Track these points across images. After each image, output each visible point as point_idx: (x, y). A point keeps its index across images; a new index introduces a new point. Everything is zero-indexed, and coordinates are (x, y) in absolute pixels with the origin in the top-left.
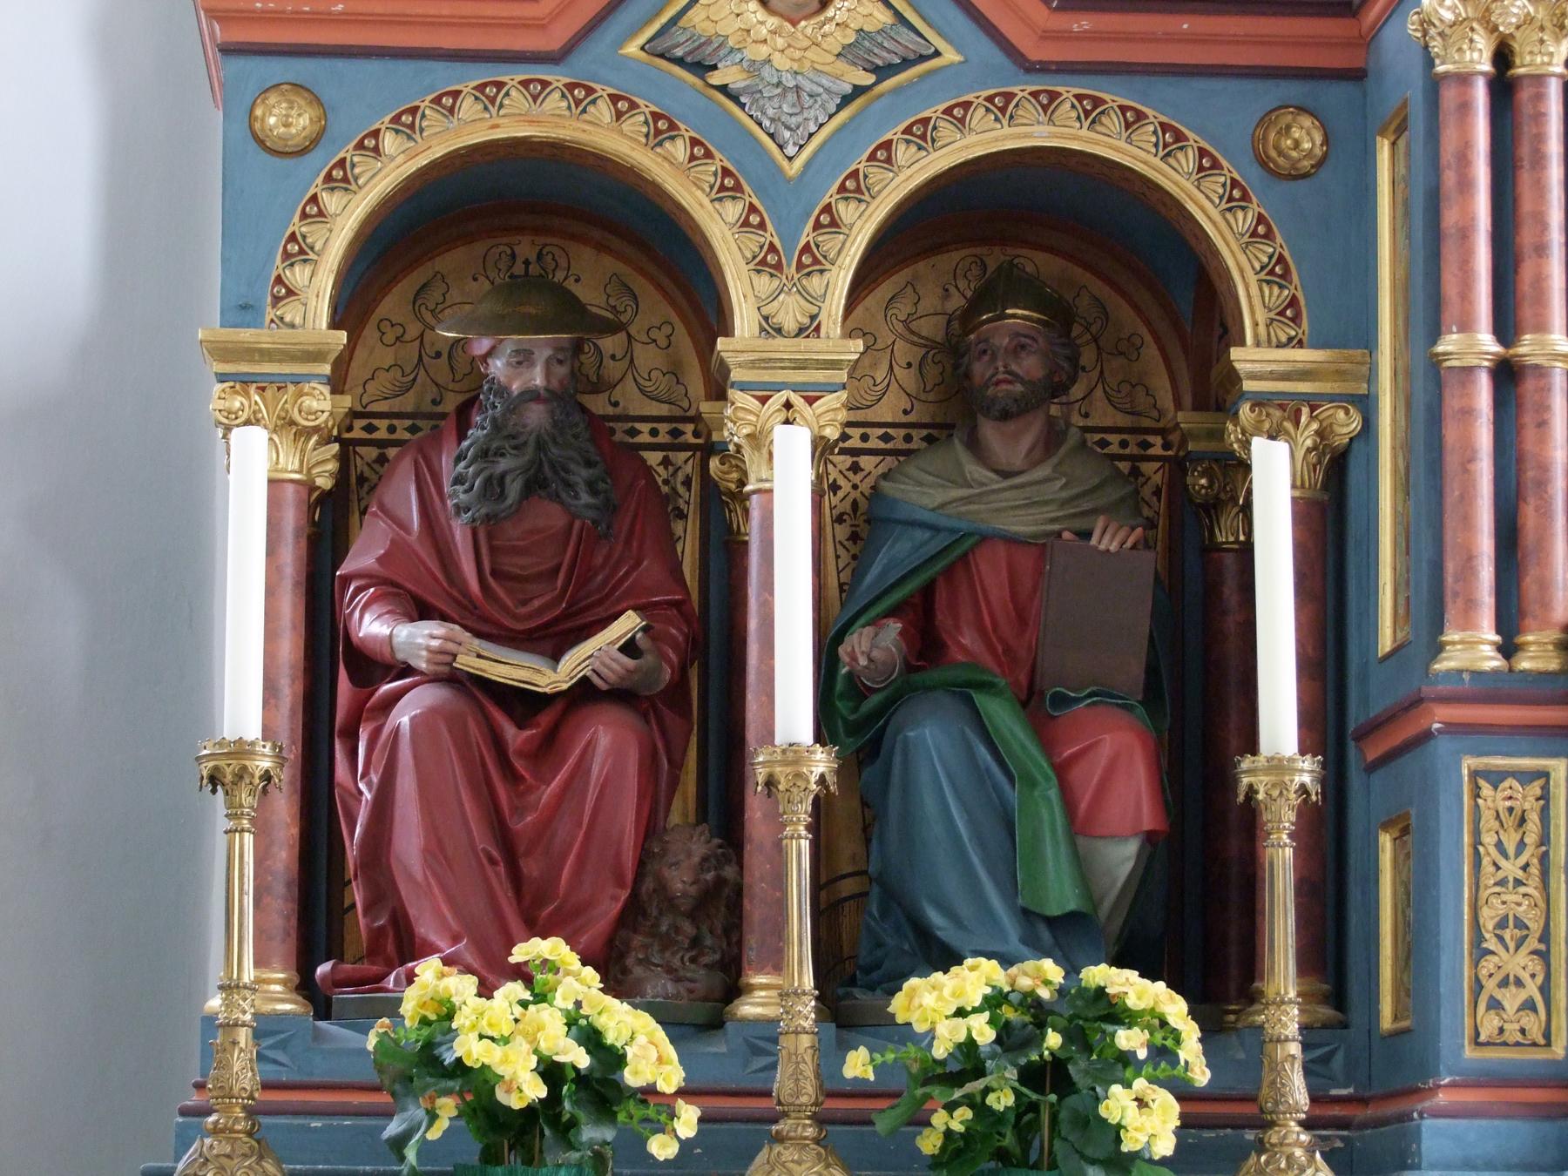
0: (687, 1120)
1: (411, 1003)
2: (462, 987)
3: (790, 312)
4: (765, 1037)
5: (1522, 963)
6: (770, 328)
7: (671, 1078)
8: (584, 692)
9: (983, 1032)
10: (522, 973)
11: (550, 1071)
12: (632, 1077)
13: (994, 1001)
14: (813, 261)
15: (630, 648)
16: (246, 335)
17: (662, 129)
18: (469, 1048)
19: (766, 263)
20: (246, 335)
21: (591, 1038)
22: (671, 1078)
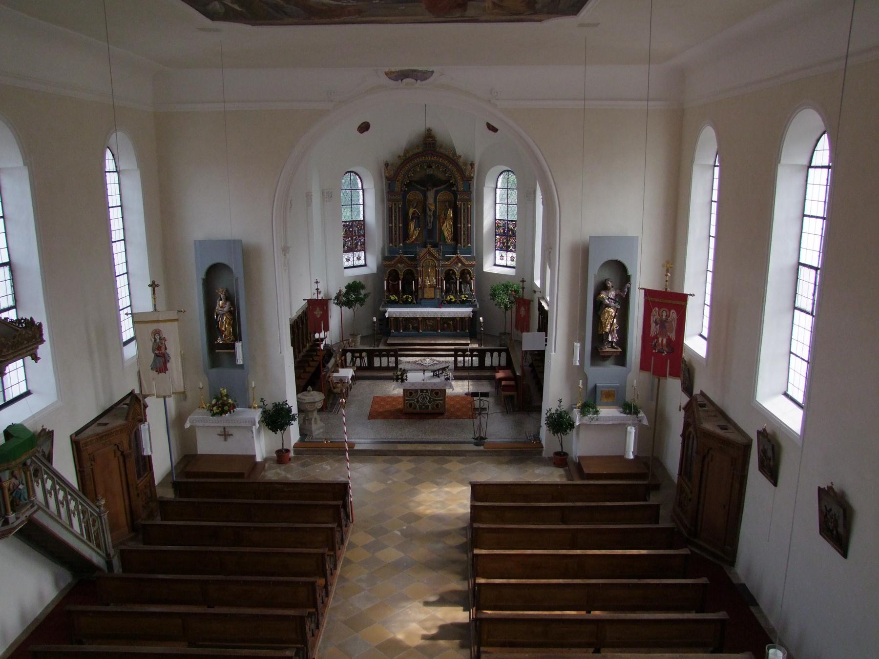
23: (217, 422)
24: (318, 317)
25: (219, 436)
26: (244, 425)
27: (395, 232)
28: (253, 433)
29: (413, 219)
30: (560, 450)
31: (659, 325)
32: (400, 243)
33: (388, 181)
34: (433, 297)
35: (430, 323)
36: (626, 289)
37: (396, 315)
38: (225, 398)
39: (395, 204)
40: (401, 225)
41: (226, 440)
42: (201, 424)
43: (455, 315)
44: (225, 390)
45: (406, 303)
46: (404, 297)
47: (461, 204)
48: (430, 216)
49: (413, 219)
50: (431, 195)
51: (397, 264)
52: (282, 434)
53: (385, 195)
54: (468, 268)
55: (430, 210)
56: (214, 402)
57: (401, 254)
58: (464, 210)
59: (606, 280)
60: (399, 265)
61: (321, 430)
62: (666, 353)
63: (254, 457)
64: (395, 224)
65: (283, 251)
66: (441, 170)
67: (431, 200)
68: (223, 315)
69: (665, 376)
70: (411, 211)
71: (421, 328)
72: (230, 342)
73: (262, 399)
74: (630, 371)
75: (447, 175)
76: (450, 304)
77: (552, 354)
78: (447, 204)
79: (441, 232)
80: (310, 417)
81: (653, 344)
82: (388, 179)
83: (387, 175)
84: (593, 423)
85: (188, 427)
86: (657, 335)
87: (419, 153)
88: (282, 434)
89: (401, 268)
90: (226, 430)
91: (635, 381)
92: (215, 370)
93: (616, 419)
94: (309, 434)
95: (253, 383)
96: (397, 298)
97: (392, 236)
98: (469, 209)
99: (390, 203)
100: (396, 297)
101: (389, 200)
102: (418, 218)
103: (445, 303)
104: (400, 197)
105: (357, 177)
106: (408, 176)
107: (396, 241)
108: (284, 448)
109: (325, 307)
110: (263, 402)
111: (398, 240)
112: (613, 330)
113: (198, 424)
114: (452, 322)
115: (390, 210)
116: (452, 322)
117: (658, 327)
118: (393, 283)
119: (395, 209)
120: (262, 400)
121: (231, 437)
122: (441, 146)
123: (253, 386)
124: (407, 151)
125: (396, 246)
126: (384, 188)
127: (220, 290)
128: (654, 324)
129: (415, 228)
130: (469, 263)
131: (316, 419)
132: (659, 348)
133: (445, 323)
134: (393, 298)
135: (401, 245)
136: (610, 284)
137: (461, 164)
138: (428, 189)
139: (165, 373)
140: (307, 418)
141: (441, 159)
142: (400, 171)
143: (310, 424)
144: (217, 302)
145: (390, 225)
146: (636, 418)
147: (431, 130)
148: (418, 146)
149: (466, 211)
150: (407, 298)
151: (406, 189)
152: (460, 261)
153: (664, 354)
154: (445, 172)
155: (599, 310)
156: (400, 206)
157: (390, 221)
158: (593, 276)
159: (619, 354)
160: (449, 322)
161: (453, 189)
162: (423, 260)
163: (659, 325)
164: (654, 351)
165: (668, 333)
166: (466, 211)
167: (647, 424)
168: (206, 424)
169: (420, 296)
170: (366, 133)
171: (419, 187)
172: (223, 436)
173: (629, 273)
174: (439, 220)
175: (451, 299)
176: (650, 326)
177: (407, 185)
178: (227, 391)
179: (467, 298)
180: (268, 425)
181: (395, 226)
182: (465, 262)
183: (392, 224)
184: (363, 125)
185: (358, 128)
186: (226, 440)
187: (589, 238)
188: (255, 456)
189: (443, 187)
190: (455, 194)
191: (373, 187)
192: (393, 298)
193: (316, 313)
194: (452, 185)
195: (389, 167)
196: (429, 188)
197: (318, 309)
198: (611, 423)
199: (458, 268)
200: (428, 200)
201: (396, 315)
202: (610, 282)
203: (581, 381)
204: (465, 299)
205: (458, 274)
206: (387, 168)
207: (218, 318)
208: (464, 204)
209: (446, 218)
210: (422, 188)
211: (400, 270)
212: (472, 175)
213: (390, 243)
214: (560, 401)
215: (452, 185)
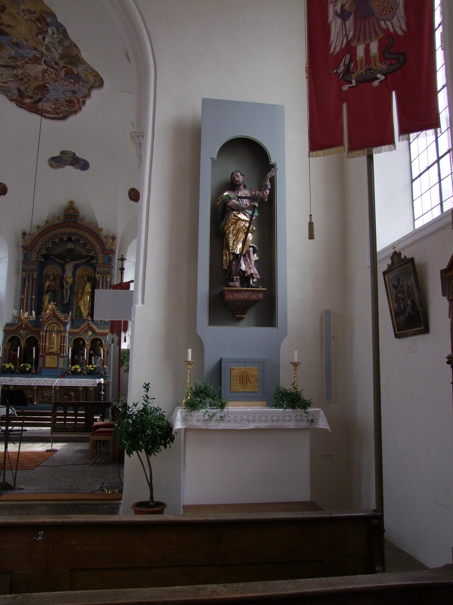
0: (13, 369)
5: (41, 364)
11: (9, 367)
14: (24, 340)
17: (19, 336)
19: (22, 340)
21: (10, 366)
27: (27, 303)
29: (47, 292)
30: (148, 499)
31: (352, 17)
33: (24, 250)
34: (56, 366)
35: (48, 394)
36: (268, 183)
39: (29, 275)
40: (34, 297)
43: (77, 384)
45: (23, 373)
46: (22, 365)
47: (100, 277)
48: (67, 290)
50: (69, 268)
51: (20, 330)
54: (100, 338)
55: (67, 283)
58: (103, 283)
59: (232, 174)
60: (22, 331)
62: (381, 77)
64: (27, 295)
66: (81, 242)
67: (69, 273)
69: (389, 141)
70: (47, 284)
71: (36, 400)
74: (285, 334)
75: (87, 248)
76: (75, 374)
77: (137, 306)
78: (86, 278)
79: (79, 308)
81: (342, 68)
82: (24, 248)
84: (212, 425)
86: (349, 42)
87: (59, 224)
89: (24, 335)
91: (296, 352)
93: (263, 419)
96: (13, 367)
98: (109, 282)
99: (24, 273)
101: (23, 270)
102: (55, 292)
103: (69, 374)
106: (46, 248)
112: (248, 252)
114: (73, 393)
115: (24, 280)
116: (73, 393)
117: (350, 23)
119: (29, 280)
122: (83, 219)
124: (47, 222)
128: (339, 21)
130: (101, 331)
132: (361, 70)
133: (65, 394)
136: (241, 179)
137: (102, 237)
138: (66, 262)
141: (82, 231)
142: (37, 241)
145: (22, 296)
146: (305, 415)
147: (73, 203)
148: (58, 218)
149: (105, 284)
150: (25, 367)
151: (43, 260)
152: (91, 329)
153: (376, 83)
154: (85, 244)
155: (222, 221)
157: (23, 293)
158: (210, 160)
159: (261, 296)
160: (71, 393)
161: (92, 262)
162: (47, 324)
163: (352, 17)
164: (345, 88)
165: (382, 23)
166: (105, 284)
167: (328, 428)
169: (40, 365)
171: (58, 260)
173: (273, 160)
174: (77, 296)
175: (76, 369)
176: (327, 29)
177: (44, 256)
179: (95, 368)
181: (27, 298)
182: (97, 330)
187: (199, 104)
189: (82, 261)
190: (94, 267)
191: (7, 256)
194: (92, 258)
195: (26, 237)
196: (68, 260)
198: (252, 426)
199: (88, 337)
200: (66, 274)
202: (239, 174)
203: (190, 351)
204: (92, 369)
205: (88, 343)
206: (24, 238)
208: (103, 277)
209: (83, 293)
210: (62, 262)
211: (22, 337)
212: (113, 248)
214: (147, 387)
215: (92, 258)
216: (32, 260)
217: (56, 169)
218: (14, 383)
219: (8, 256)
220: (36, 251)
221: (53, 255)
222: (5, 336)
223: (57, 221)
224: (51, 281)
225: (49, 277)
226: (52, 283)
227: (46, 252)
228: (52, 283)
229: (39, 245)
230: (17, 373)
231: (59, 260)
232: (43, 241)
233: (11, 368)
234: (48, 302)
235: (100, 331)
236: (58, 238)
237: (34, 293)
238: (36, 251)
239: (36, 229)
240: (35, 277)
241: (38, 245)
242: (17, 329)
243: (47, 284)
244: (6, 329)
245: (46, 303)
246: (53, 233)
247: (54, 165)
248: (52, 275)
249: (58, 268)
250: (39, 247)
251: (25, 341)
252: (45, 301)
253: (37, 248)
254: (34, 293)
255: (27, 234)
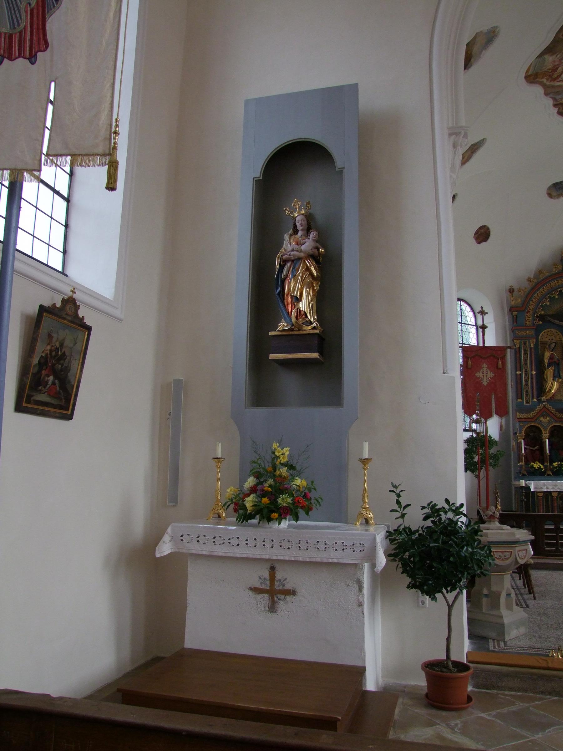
0: (544, 470)
1: (531, 464)
2: (533, 464)
3: (545, 432)
4: (547, 466)
6: (544, 433)
7: (543, 468)
8: (536, 450)
9: (557, 465)
10: (536, 463)
12: (541, 468)
13: (557, 464)
14: (546, 430)
15: (538, 448)
16: (520, 434)
17: (539, 424)
18: (535, 467)
20: (521, 434)
21: (539, 466)
22: (543, 468)
23: (252, 543)
24: (485, 383)
25: (250, 593)
26: (335, 557)
27: (526, 381)
28: (361, 589)
29: (550, 365)
32: (533, 397)
37: (547, 488)
38: (284, 471)
39: (525, 343)
40: (534, 372)
41: (272, 608)
42: (204, 550)
44: (286, 451)
49: (550, 365)
52: (450, 607)
53: (508, 335)
56: (251, 482)
57: (544, 402)
60: (542, 419)
61: (522, 630)
63: (360, 671)
64: (526, 371)
65: (450, 135)
68: (295, 261)
70: (547, 354)
72: (312, 332)
73: (488, 313)
80: (494, 588)
83: (513, 303)
85: (166, 553)
88: (450, 607)
90: (279, 575)
92: (262, 412)
94: (493, 635)
95: (366, 445)
96: (542, 467)
97: (521, 389)
99: (518, 341)
100: (541, 465)
102: (558, 364)
104: (533, 332)
105: (468, 309)
107: (527, 395)
108: (453, 657)
109: (500, 362)
110: (399, 496)
111: (530, 393)
113: (195, 548)
118: (532, 449)
119: (525, 350)
120: (395, 490)
121: (288, 598)
123: (366, 455)
125: (527, 402)
126: (507, 323)
127: (297, 203)
129: (554, 378)
131: (508, 595)
134: (537, 465)
135: (535, 400)
139: (32, 59)
140: (485, 591)
143: (496, 605)
144: (286, 237)
145: (518, 373)
148: (555, 265)
151: (541, 323)
156: (532, 346)
168: (221, 551)
170: (484, 243)
171: (557, 322)
172: (266, 596)
177: (541, 318)
178: (290, 456)
180: (408, 570)
181: (526, 374)
183: (521, 370)
184: (482, 231)
185: (475, 234)
186: (272, 608)
188: (364, 669)
192: (537, 465)
193: (479, 374)
195: (515, 293)
197: (485, 366)
201: (547, 488)
207: (285, 270)
211: (543, 426)
213: (517, 398)
216: (526, 323)
217: (555, 199)
218: (559, 488)
219: (494, 321)
220: (530, 312)
221: (549, 315)
222: (521, 426)
223: (554, 270)
224: (551, 350)
225: (549, 346)
226: (552, 353)
227: (543, 312)
228: (552, 353)
229: (533, 304)
230: (549, 475)
231: (558, 322)
232: (537, 297)
233: (540, 468)
234: (553, 379)
235: (521, 415)
236: (557, 292)
237: (533, 367)
238: (530, 312)
239: (527, 282)
240: (533, 347)
241: (531, 303)
242: (535, 416)
243: (547, 354)
244: (521, 416)
245: (550, 379)
246: (550, 286)
247: (554, 194)
248: (553, 343)
249: (557, 332)
250: (533, 306)
251: (548, 431)
252: (547, 378)
253: (531, 307)
254: (533, 367)
255: (516, 290)
